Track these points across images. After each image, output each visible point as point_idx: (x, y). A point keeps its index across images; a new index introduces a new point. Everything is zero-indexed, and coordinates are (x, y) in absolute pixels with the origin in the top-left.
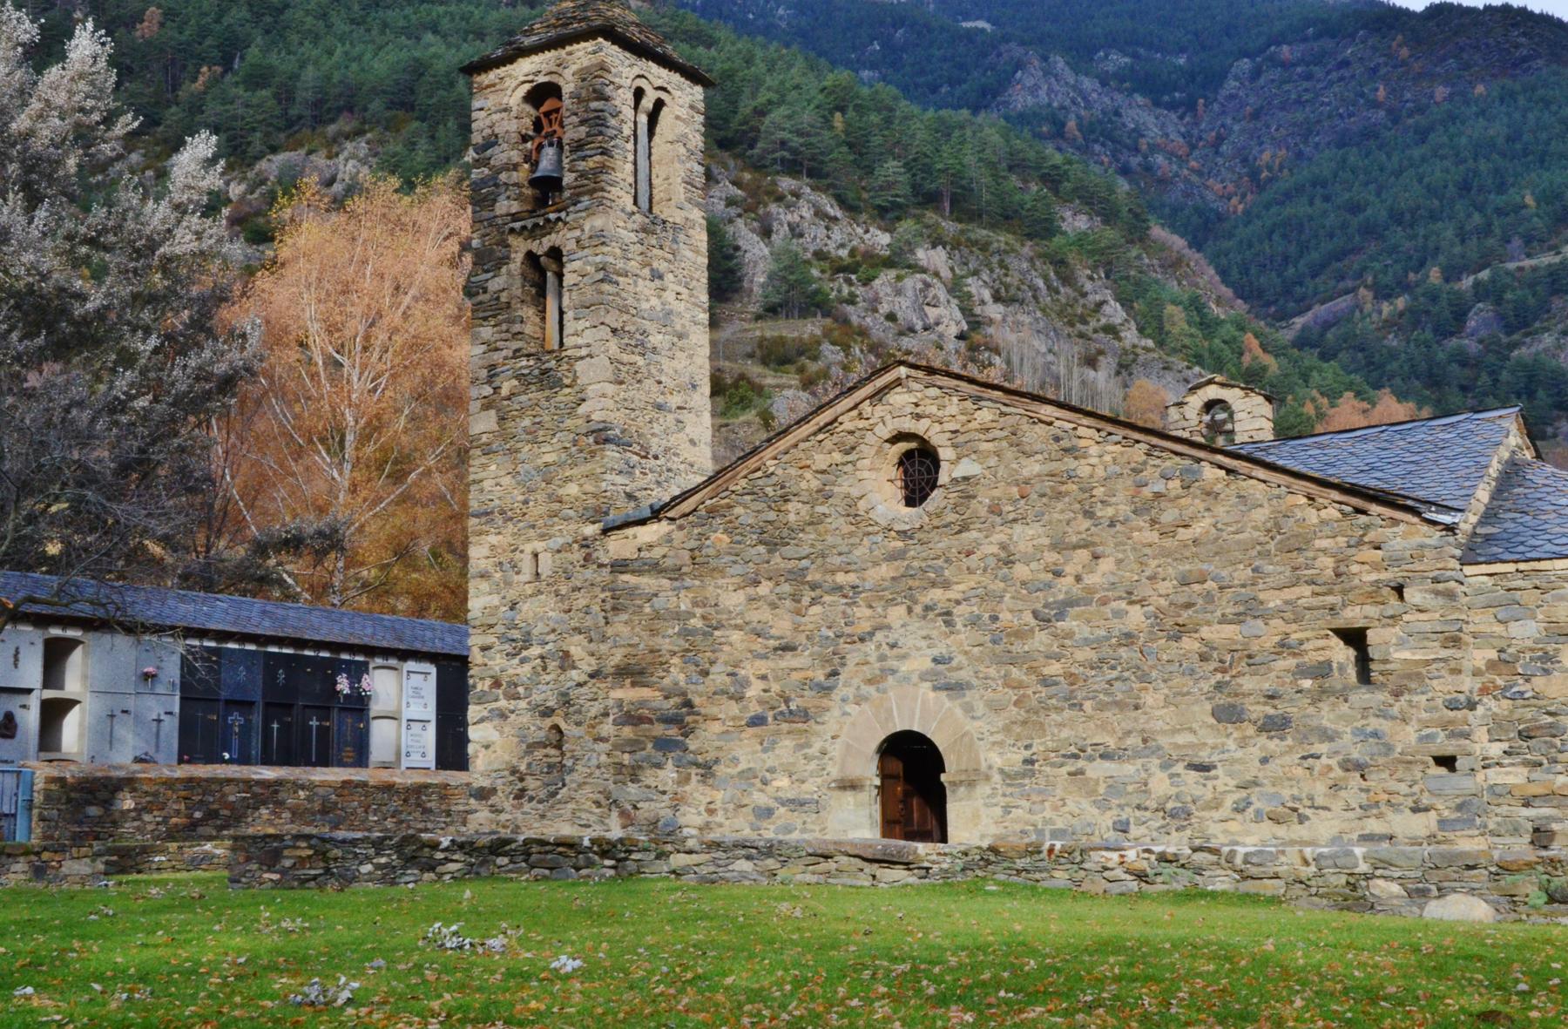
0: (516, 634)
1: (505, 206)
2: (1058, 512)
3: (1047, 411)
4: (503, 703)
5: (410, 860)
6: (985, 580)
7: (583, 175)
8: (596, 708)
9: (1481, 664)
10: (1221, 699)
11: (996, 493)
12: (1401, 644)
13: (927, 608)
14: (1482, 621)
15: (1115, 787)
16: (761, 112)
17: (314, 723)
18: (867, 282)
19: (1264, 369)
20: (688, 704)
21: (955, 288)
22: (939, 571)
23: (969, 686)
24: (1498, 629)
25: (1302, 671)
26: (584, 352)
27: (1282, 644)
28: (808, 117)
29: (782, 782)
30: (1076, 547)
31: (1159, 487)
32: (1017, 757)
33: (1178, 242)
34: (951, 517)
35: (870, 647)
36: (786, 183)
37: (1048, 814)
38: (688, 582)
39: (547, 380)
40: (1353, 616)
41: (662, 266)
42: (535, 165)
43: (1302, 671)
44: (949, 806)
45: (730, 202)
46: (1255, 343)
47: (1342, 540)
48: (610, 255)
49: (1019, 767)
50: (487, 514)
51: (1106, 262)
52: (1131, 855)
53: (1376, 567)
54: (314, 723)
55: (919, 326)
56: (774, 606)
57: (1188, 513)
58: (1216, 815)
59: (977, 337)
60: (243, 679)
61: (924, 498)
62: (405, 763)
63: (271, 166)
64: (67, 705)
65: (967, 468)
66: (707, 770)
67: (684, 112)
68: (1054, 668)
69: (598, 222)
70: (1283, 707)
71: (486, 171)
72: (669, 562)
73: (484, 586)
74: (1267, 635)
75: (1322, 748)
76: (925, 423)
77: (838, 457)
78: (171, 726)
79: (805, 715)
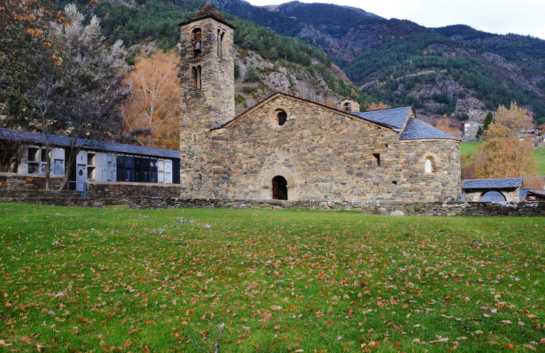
0: (190, 153)
1: (187, 56)
2: (314, 127)
3: (311, 104)
4: (188, 169)
5: (169, 203)
6: (297, 142)
7: (206, 49)
8: (209, 170)
9: (403, 162)
10: (348, 169)
11: (300, 123)
12: (387, 157)
13: (284, 148)
14: (403, 152)
15: (325, 188)
16: (244, 36)
17: (146, 173)
18: (268, 75)
19: (356, 96)
20: (230, 169)
21: (288, 77)
22: (286, 140)
23: (293, 166)
24: (407, 154)
25: (366, 163)
27: (362, 157)
28: (255, 37)
29: (251, 187)
30: (317, 135)
31: (336, 122)
32: (303, 181)
33: (337, 68)
34: (289, 128)
35: (271, 157)
36: (250, 52)
37: (310, 194)
38: (230, 142)
39: (198, 96)
40: (377, 151)
41: (224, 70)
42: (195, 47)
43: (366, 163)
44: (288, 192)
45: (237, 56)
46: (354, 91)
47: (375, 134)
48: (212, 67)
49: (304, 184)
51: (321, 71)
52: (329, 203)
53: (382, 140)
54: (146, 173)
55: (280, 85)
56: (249, 147)
57: (342, 128)
58: (347, 194)
59: (293, 88)
60: (130, 163)
61: (283, 124)
62: (166, 182)
63: (133, 48)
64: (93, 168)
65: (293, 117)
66: (234, 184)
67: (229, 35)
68: (312, 162)
69: (209, 60)
70: (361, 171)
72: (225, 137)
73: (183, 142)
74: (358, 155)
75: (369, 180)
76: (284, 106)
77: (264, 114)
78: (115, 174)
79: (256, 172)
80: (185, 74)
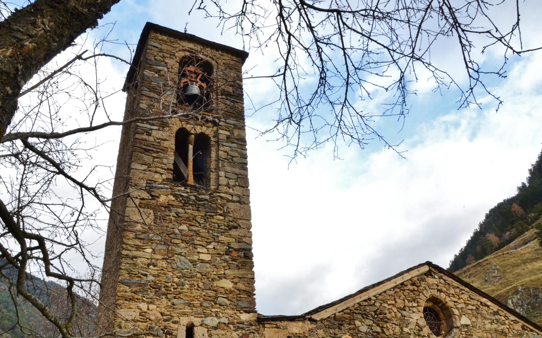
26: (235, 198)
50: (140, 285)
65: (465, 320)
71: (157, 75)
80: (157, 134)
